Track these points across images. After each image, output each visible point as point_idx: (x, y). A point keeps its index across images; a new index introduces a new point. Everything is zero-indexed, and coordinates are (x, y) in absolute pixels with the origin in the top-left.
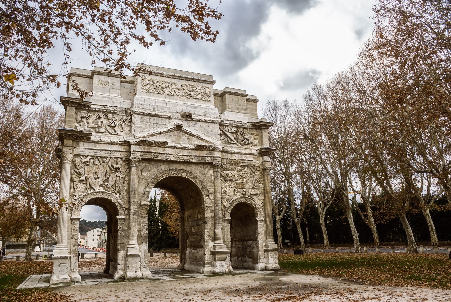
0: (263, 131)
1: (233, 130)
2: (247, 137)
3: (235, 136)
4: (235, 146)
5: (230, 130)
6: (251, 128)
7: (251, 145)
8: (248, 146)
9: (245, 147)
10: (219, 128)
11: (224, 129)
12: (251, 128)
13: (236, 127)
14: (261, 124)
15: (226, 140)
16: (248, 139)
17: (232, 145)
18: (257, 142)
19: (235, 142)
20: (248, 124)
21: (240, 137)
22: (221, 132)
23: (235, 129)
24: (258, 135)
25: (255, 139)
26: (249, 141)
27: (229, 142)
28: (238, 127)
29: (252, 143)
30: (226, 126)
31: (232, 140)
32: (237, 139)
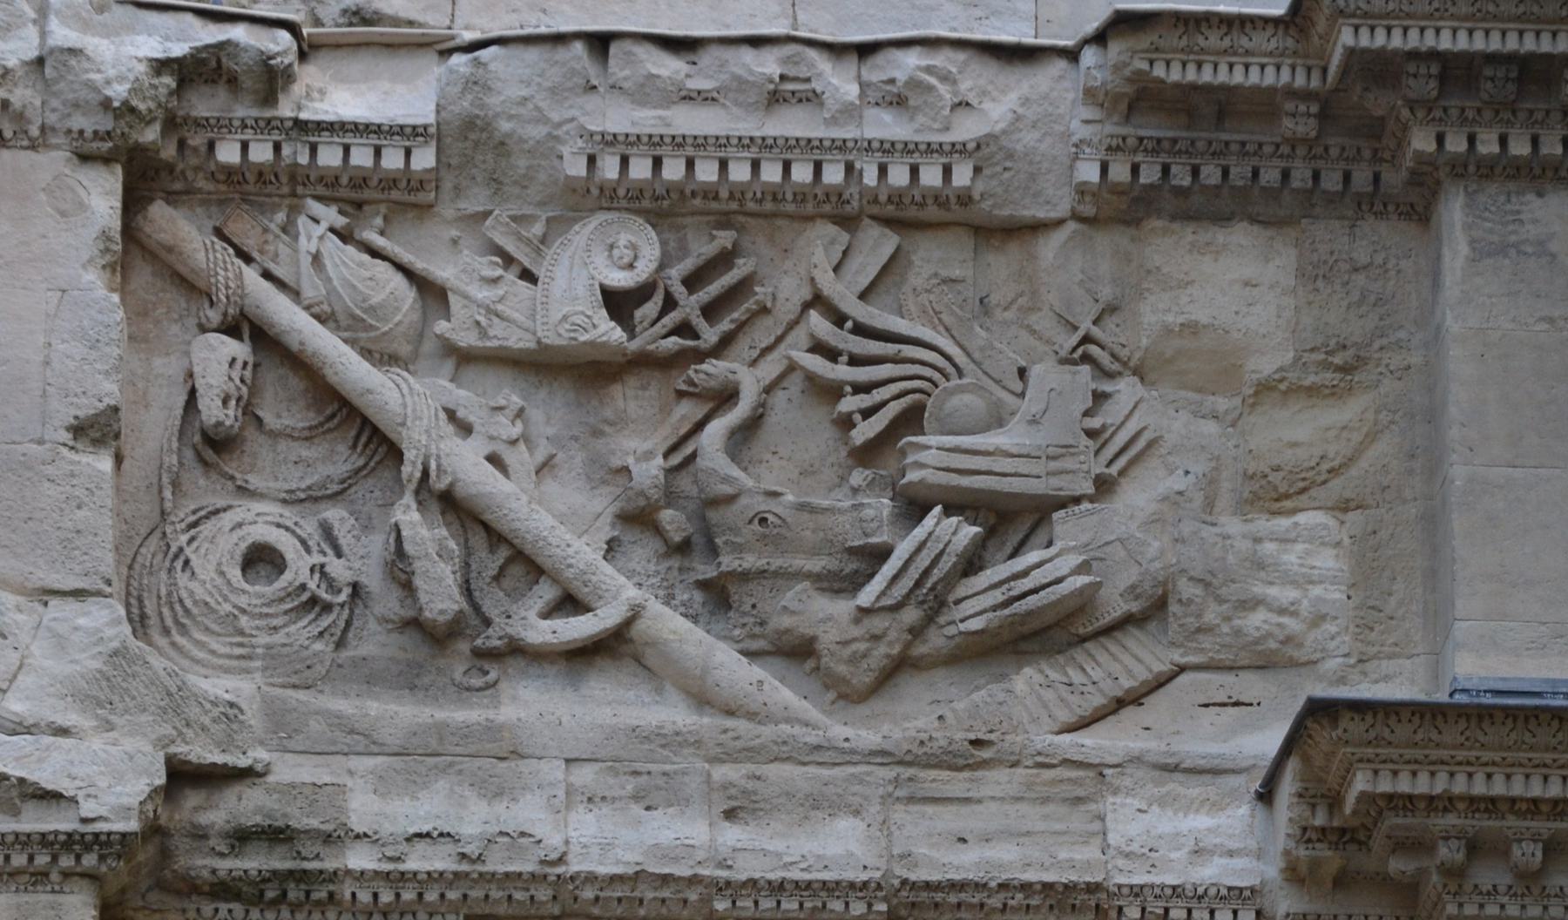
0: (1456, 252)
1: (572, 288)
2: (1011, 447)
3: (642, 454)
4: (609, 705)
5: (487, 306)
6: (1120, 209)
7: (1137, 658)
8: (1030, 698)
9: (925, 712)
10: (133, 249)
11: (317, 278)
12: (1120, 209)
13: (661, 207)
14: (1377, 69)
15: (362, 561)
16: (1009, 519)
17: (527, 703)
18: (1305, 564)
19: (621, 591)
20: (1000, 102)
21: (794, 478)
22: (218, 359)
23: (623, 252)
24: (1338, 368)
25: (1274, 493)
26: (1052, 566)
27: (471, 621)
28: (714, 225)
29: (1152, 611)
30: (357, 196)
31: (524, 563)
32: (683, 531)
